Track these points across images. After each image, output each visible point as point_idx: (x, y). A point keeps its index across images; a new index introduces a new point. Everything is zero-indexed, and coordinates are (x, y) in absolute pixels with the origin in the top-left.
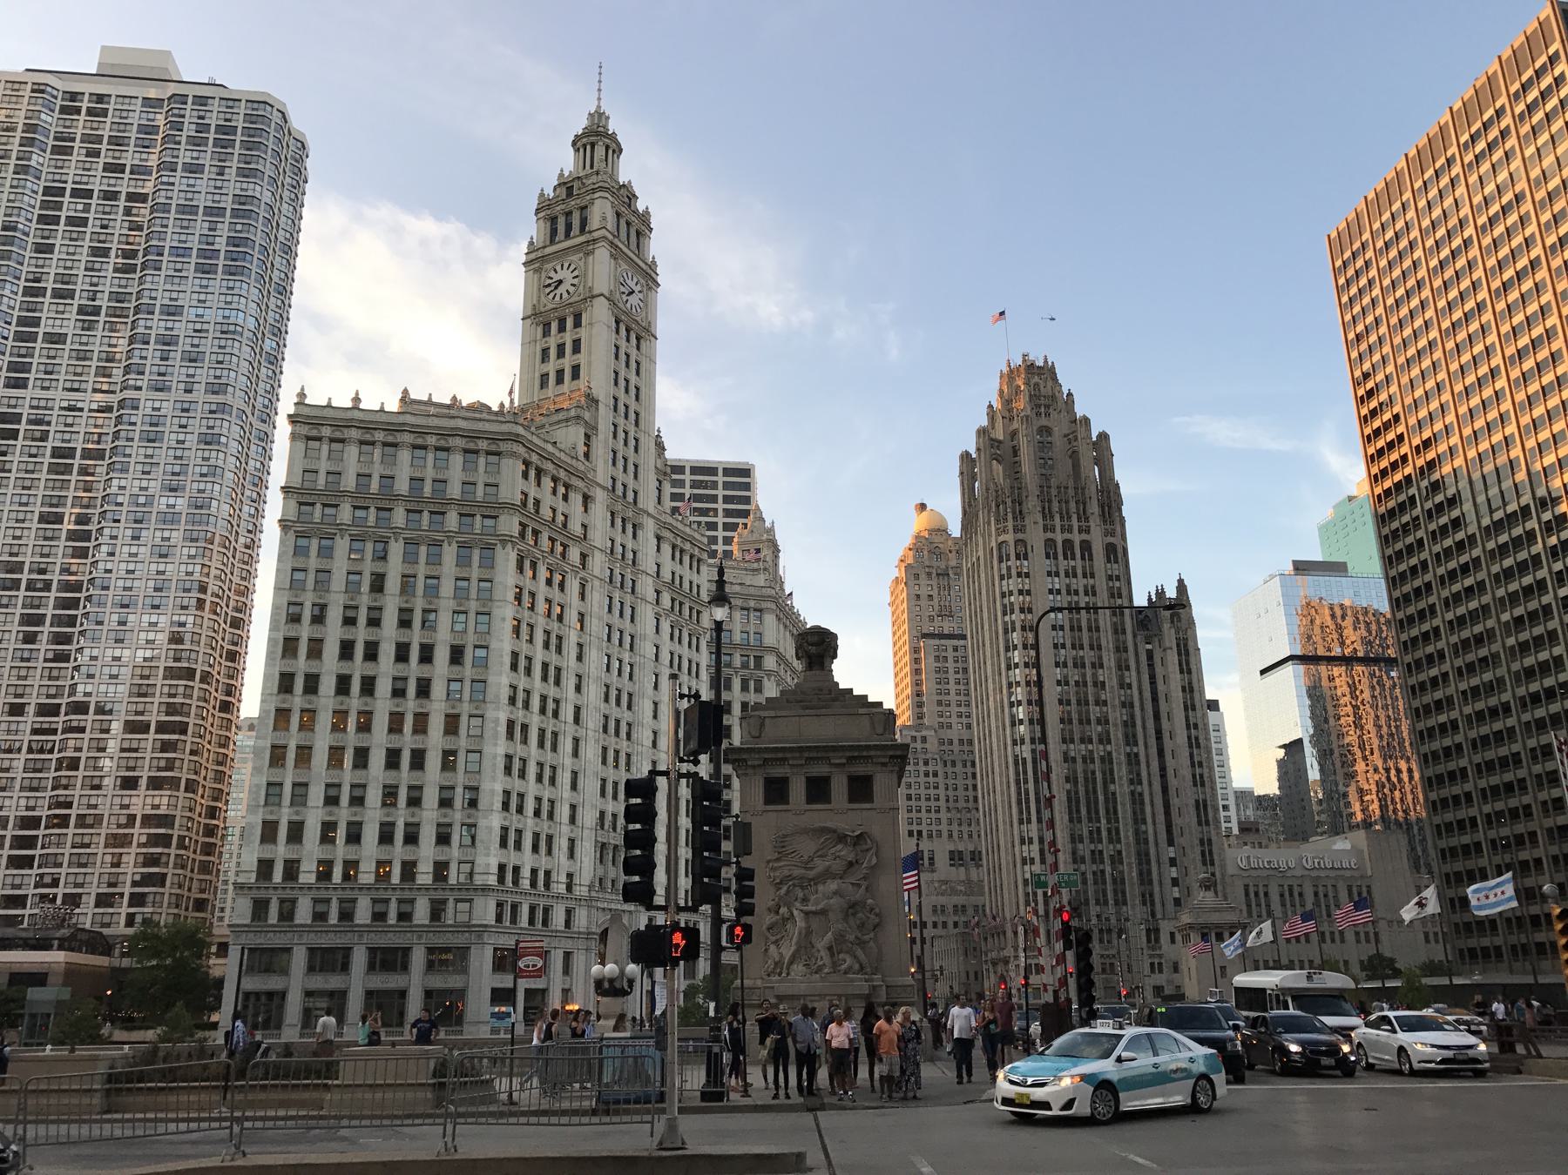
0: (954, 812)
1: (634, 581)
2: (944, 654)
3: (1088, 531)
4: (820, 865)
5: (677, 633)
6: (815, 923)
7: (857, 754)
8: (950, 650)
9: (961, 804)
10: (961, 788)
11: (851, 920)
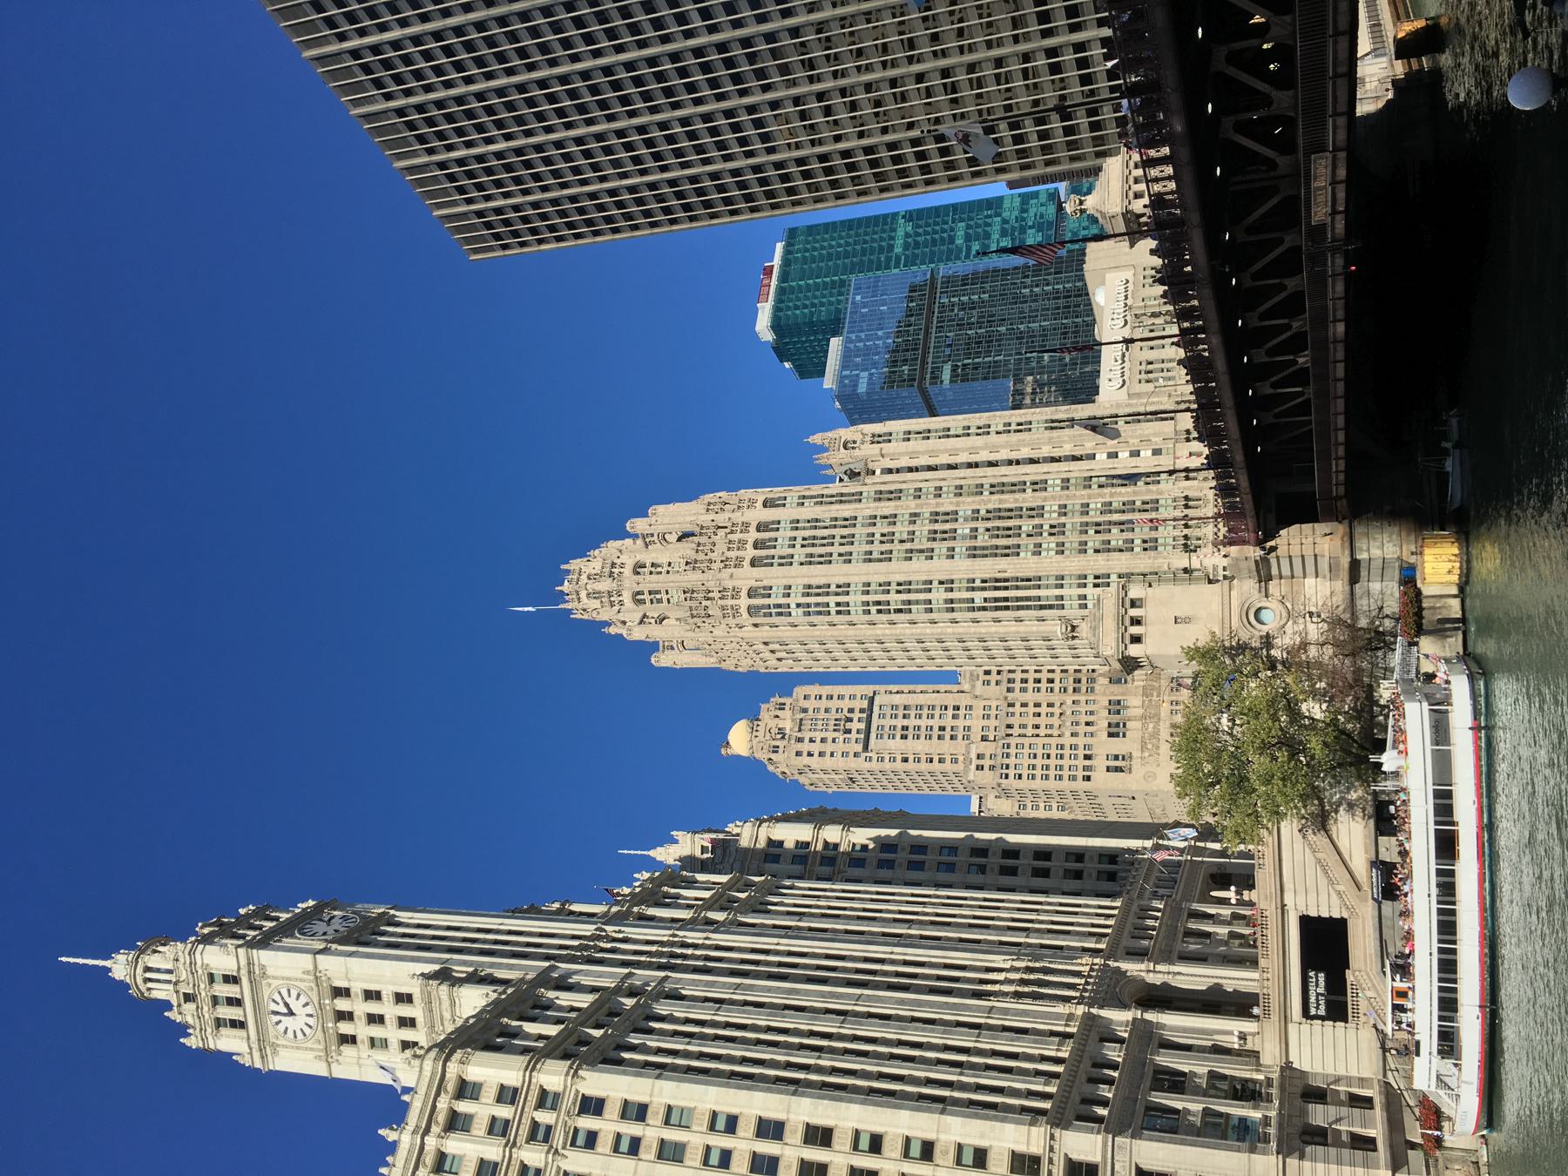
0: (1063, 729)
2: (887, 729)
3: (746, 525)
8: (882, 722)
9: (1055, 721)
10: (1037, 721)
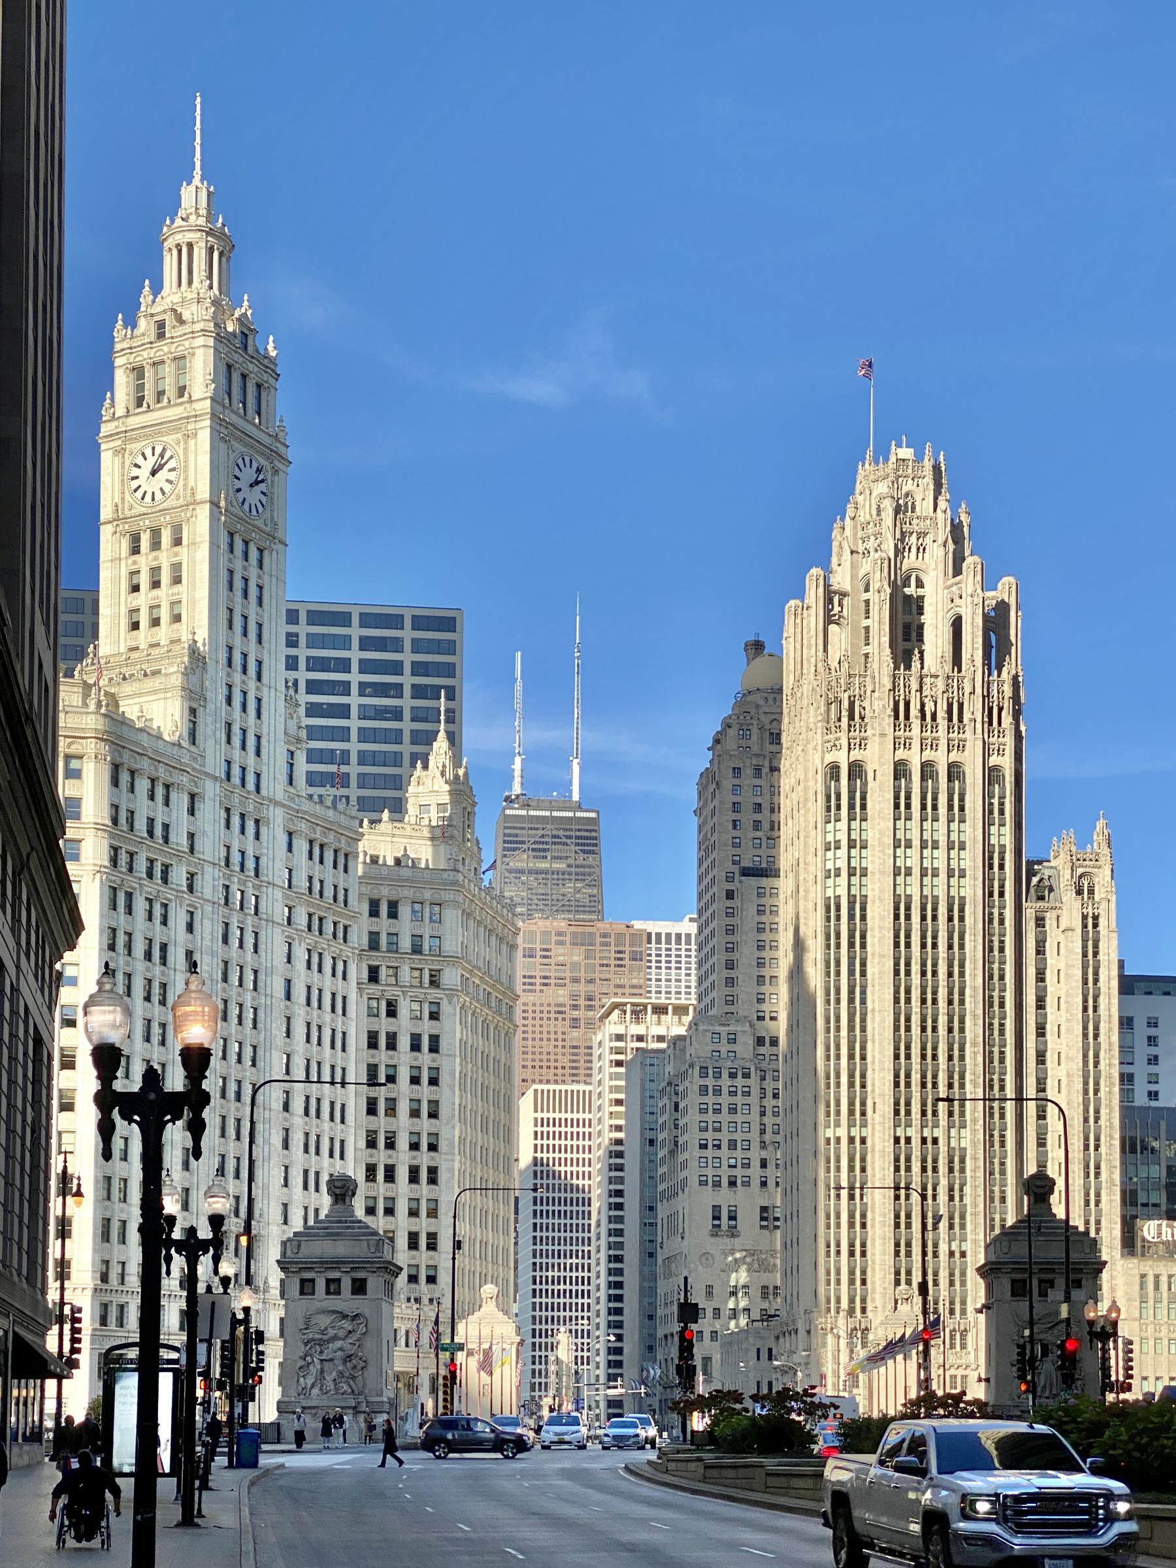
1: (257, 897)
4: (331, 1332)
5: (315, 960)
6: (326, 1365)
7: (356, 1265)
11: (349, 1364)
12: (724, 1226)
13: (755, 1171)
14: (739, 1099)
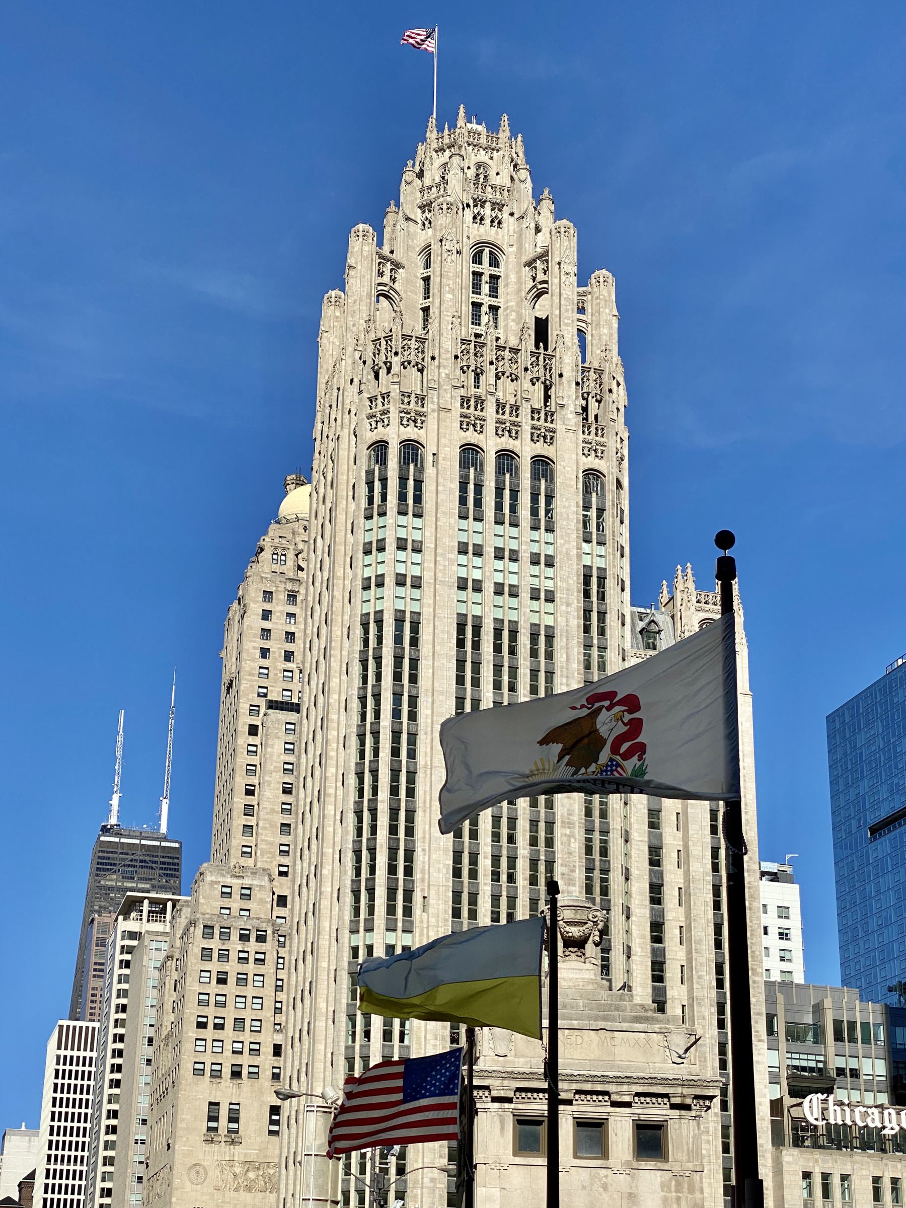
3: (549, 437)
12: (223, 1131)
13: (266, 1060)
14: (251, 968)
